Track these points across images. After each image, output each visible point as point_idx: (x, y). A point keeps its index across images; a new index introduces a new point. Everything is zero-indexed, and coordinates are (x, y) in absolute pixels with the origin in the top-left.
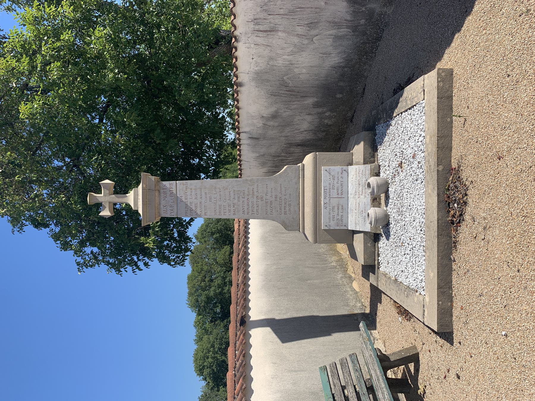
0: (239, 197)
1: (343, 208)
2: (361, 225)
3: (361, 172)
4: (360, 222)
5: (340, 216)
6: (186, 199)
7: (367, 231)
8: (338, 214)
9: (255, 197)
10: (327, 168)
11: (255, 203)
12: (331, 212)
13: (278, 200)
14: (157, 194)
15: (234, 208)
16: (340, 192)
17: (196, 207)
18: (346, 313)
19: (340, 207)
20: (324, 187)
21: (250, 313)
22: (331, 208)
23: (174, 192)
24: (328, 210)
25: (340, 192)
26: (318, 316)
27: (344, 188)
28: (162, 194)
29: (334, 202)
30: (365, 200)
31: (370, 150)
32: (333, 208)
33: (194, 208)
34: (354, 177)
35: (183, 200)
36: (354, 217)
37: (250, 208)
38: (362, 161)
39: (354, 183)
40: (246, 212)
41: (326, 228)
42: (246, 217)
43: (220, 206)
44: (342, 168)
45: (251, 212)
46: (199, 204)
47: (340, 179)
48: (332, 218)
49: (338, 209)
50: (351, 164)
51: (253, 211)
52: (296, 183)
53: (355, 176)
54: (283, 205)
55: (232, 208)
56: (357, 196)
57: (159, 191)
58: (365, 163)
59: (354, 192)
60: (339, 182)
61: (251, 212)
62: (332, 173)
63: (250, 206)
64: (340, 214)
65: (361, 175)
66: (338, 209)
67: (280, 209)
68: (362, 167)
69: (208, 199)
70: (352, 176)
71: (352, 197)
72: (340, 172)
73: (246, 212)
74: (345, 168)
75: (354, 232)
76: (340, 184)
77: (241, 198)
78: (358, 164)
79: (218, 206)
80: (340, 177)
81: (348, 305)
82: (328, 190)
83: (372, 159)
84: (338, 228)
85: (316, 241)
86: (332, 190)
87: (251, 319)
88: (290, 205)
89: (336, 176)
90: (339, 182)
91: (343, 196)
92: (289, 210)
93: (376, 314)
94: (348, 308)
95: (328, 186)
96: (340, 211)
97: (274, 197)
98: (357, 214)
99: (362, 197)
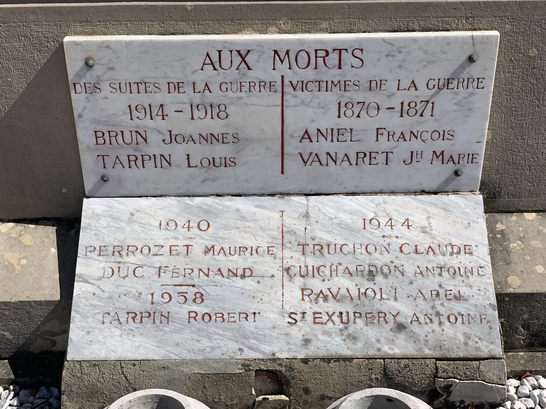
1: (214, 167)
2: (108, 286)
3: (452, 285)
4: (138, 286)
5: (165, 150)
7: (76, 334)
8: (173, 138)
10: (488, 68)
12: (188, 96)
16: (323, 146)
19: (220, 151)
20: (357, 51)
24: (200, 78)
25: (323, 146)
27: (346, 174)
29: (256, 114)
30: (271, 316)
32: (217, 110)
38: (516, 285)
39: (374, 235)
41: (73, 66)
44: (472, 158)
47: (403, 149)
48: (144, 99)
49: (211, 138)
50: (496, 202)
53: (424, 242)
56: (294, 258)
58: (507, 302)
59: (323, 236)
60: (384, 144)
62: (445, 101)
64: (178, 152)
65: (430, 283)
68: (482, 292)
72: (450, 147)
74: (476, 172)
75: (68, 229)
76: (369, 144)
78: (497, 243)
80: (416, 145)
82: (333, 75)
83: (522, 336)
84: (85, 137)
86: (331, 98)
89: (428, 124)
90: (384, 144)
91: (293, 165)
95: (364, 74)
96: (199, 152)
98: (181, 262)
99: (292, 296)
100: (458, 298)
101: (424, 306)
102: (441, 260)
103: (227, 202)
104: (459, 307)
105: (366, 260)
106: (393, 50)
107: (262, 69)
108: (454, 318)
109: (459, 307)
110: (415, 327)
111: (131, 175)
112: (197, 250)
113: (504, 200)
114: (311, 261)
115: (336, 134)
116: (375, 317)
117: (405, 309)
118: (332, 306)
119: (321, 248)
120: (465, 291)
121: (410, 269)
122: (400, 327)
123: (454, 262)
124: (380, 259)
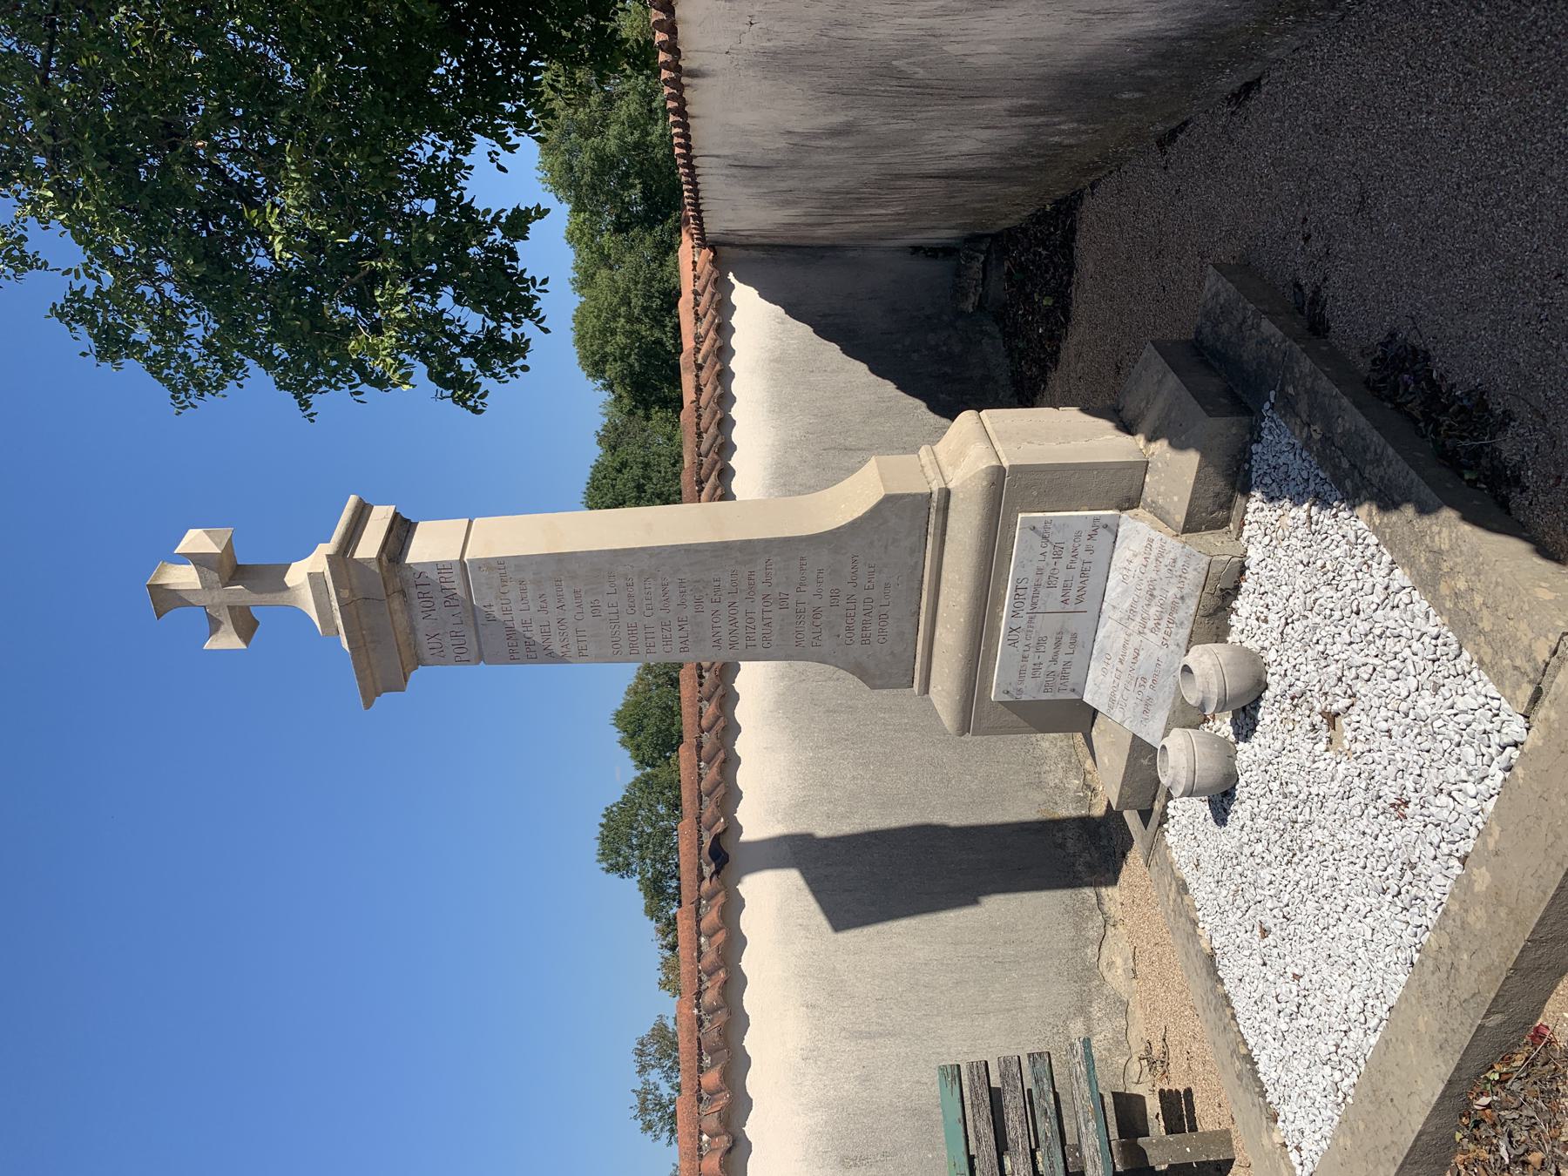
0: (699, 601)
2: (1128, 714)
3: (1167, 560)
6: (506, 612)
8: (1054, 660)
9: (758, 598)
11: (758, 616)
12: (1031, 654)
13: (843, 602)
14: (396, 604)
15: (683, 633)
16: (1073, 594)
17: (546, 634)
18: (1029, 814)
19: (1066, 639)
21: (743, 814)
22: (1033, 642)
23: (461, 592)
25: (1073, 594)
26: (942, 828)
28: (416, 602)
29: (1047, 625)
31: (1220, 484)
32: (1041, 642)
33: (538, 639)
34: (1139, 561)
35: (497, 614)
36: (1110, 679)
37: (742, 631)
39: (1132, 581)
40: (725, 642)
41: (1007, 698)
42: (725, 655)
43: (632, 630)
45: (742, 642)
46: (554, 624)
48: (1029, 672)
49: (1058, 644)
51: (748, 638)
52: (912, 551)
54: (859, 618)
55: (676, 633)
56: (1134, 626)
57: (403, 592)
59: (1126, 606)
60: (1078, 565)
61: (742, 642)
62: (1054, 539)
63: (741, 622)
64: (1062, 658)
65: (1164, 570)
66: (1058, 644)
67: (849, 629)
68: (1174, 546)
69: (587, 608)
70: (1128, 554)
71: (1117, 615)
73: (725, 642)
76: (1077, 572)
77: (707, 603)
79: (624, 633)
80: (1081, 550)
81: (1040, 785)
82: (1030, 592)
83: (1221, 514)
85: (964, 728)
86: (1043, 591)
87: (743, 838)
88: (883, 617)
90: (1078, 565)
91: (1081, 607)
92: (882, 630)
93: (1124, 856)
94: (1039, 797)
95: (1032, 577)
96: (1065, 648)
97: (826, 595)
98: (1124, 677)
100: (1175, 561)
101: (1174, 580)
102: (1152, 557)
103: (1098, 639)
104: (1180, 564)
105: (1143, 593)
106: (1021, 565)
107: (1023, 622)
108: (1184, 570)
109: (1180, 564)
110: (1185, 592)
111: (1072, 679)
112: (1120, 666)
113: (1133, 494)
114: (1138, 619)
115: (1066, 588)
116: (1174, 608)
117: (1173, 591)
118: (1164, 623)
119: (1132, 610)
120: (1172, 555)
121: (1154, 575)
122: (1182, 598)
123: (1155, 552)
124: (1145, 586)
